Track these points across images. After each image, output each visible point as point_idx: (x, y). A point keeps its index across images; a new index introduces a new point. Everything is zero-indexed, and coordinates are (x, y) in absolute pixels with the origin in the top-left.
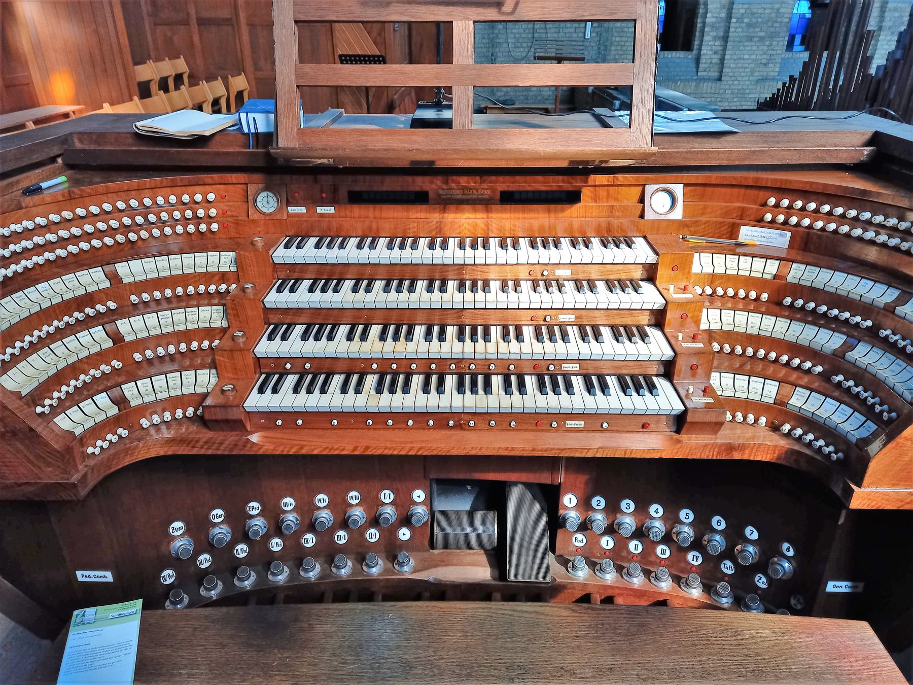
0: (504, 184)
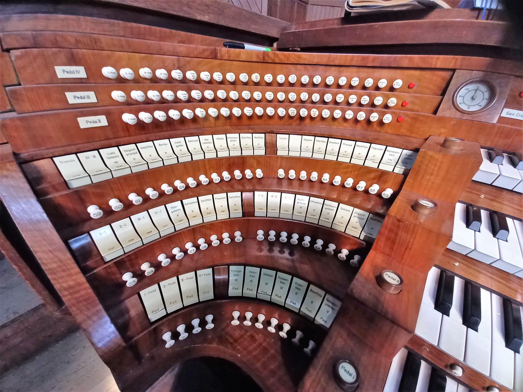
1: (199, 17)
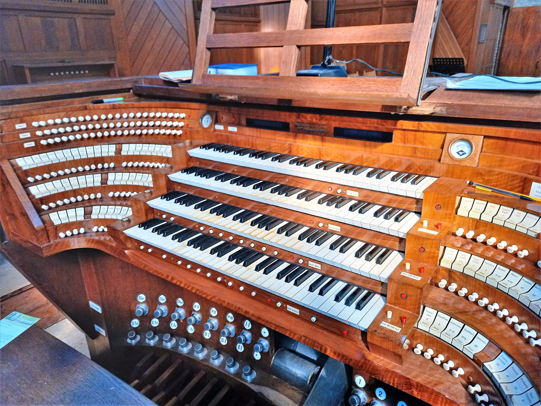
0: (336, 122)
1: (77, 92)
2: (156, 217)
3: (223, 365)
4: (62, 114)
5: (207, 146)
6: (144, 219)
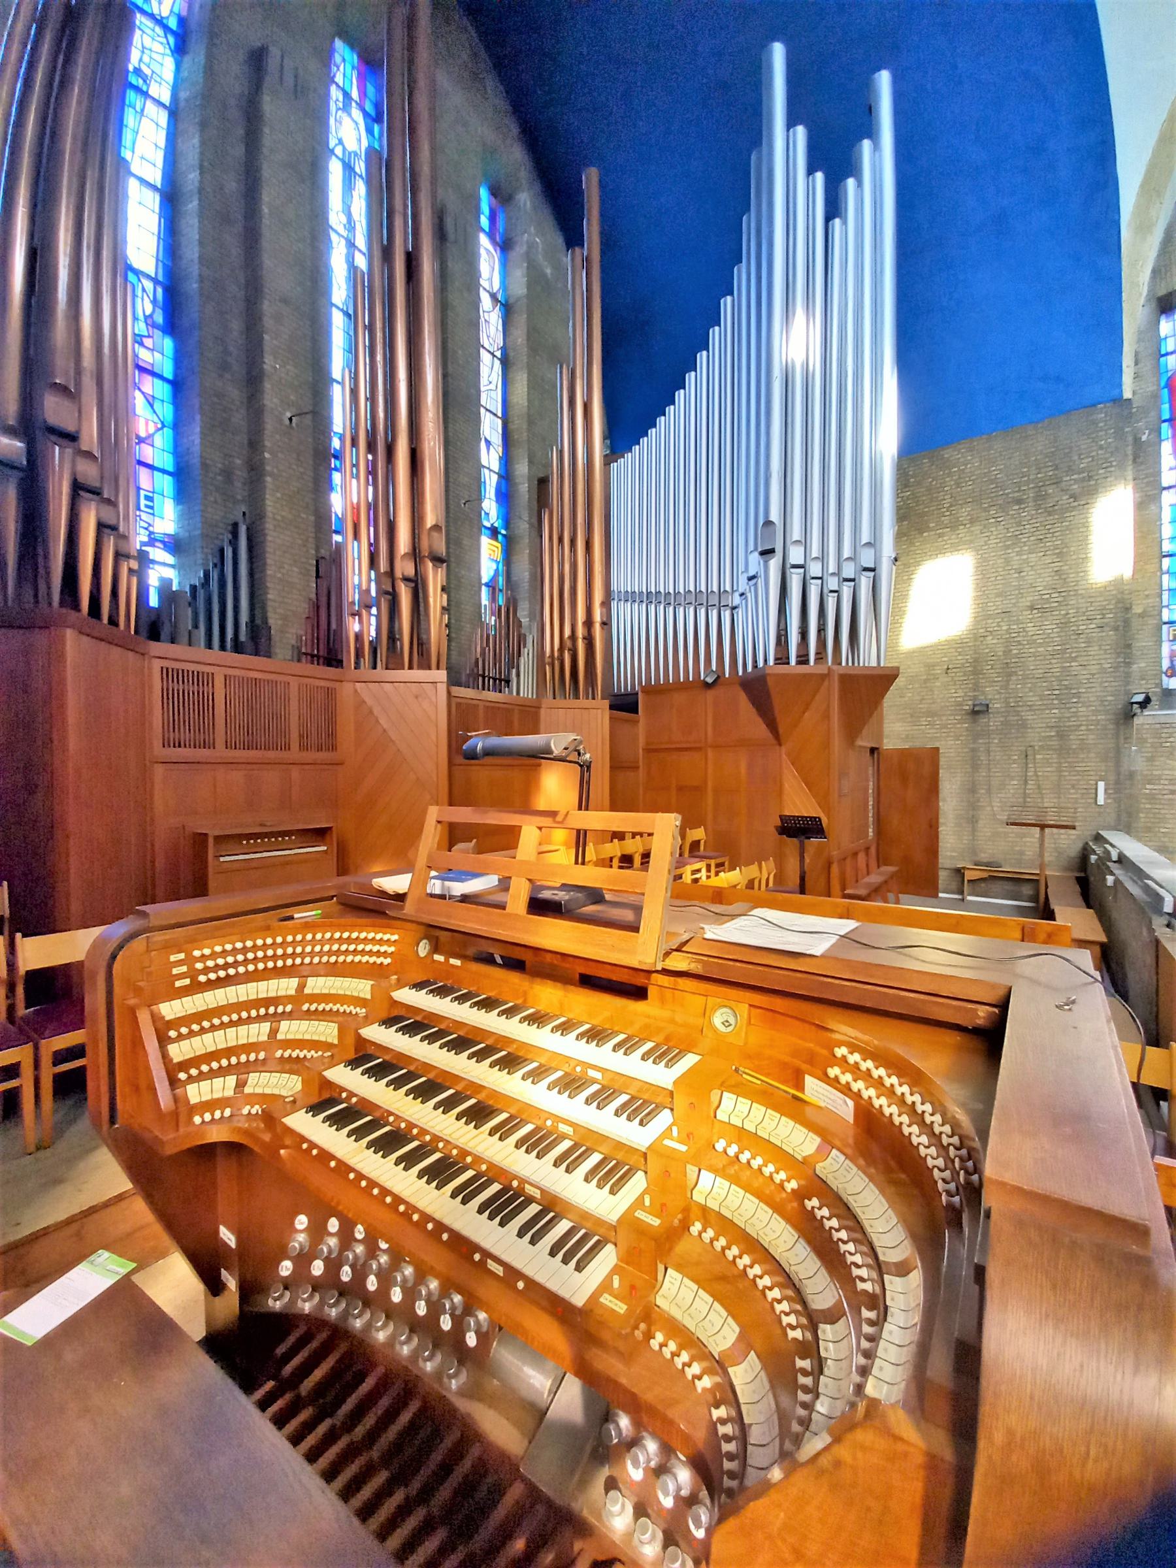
2: (336, 1095)
3: (415, 1355)
4: (234, 938)
5: (419, 986)
6: (315, 1100)
